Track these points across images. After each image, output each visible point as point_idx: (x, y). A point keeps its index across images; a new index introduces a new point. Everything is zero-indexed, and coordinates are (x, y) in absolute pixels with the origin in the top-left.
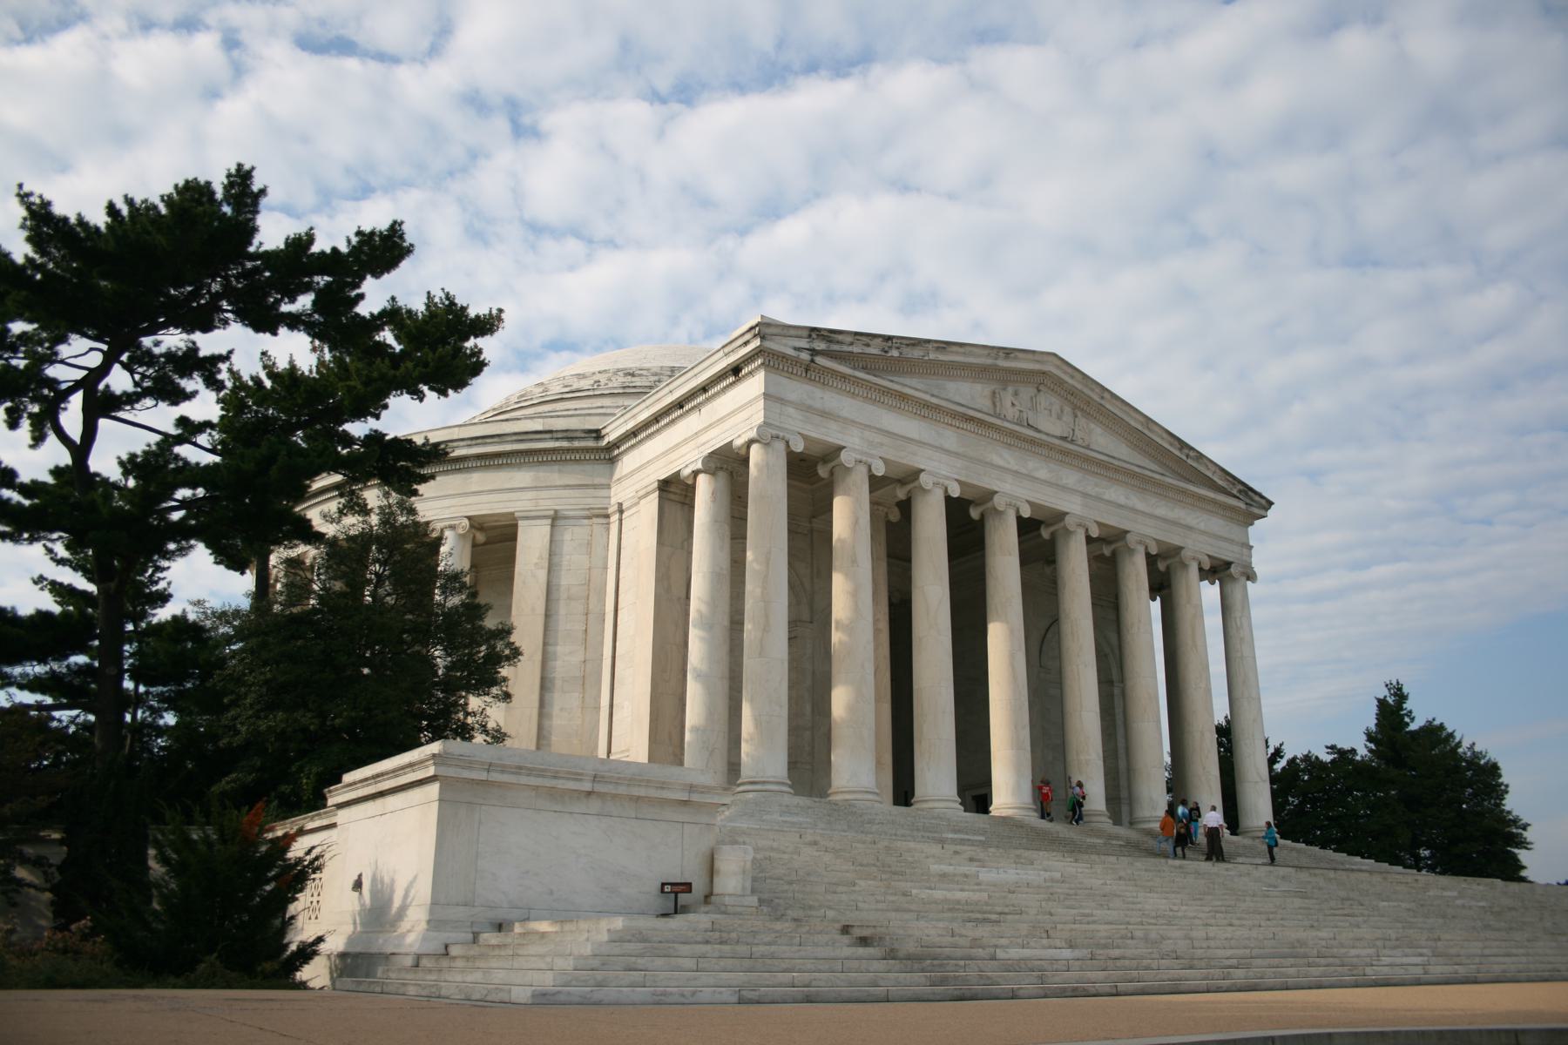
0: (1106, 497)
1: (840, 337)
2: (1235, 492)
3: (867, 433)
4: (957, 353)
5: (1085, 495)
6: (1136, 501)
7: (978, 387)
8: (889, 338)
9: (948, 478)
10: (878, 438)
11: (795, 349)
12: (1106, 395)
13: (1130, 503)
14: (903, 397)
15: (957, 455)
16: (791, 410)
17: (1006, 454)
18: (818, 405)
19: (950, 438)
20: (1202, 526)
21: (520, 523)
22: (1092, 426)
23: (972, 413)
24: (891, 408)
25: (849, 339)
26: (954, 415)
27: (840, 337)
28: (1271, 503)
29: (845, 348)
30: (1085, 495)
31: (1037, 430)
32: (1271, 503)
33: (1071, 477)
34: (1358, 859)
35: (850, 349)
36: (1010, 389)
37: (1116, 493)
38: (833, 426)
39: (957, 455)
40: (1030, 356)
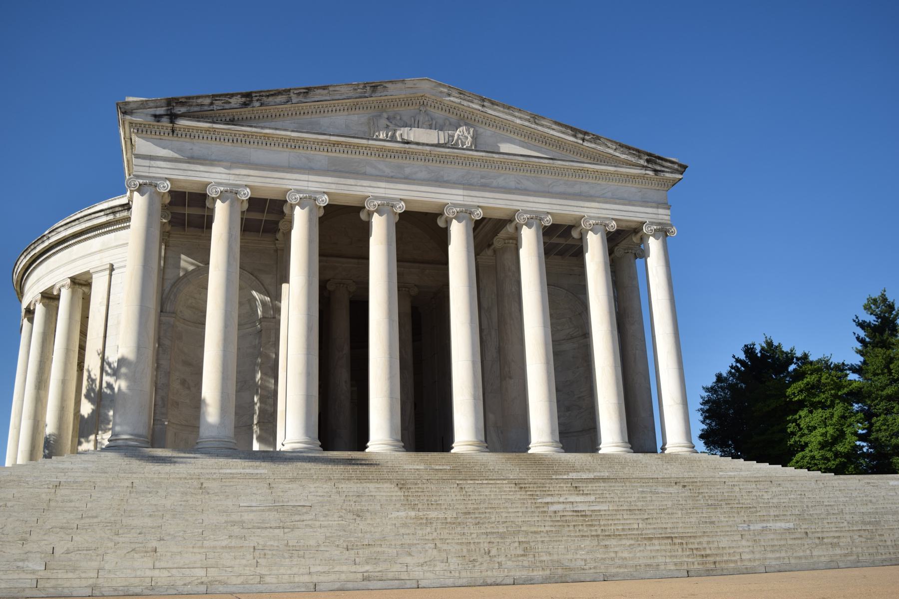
0: (495, 184)
1: (199, 101)
2: (642, 162)
4: (320, 94)
8: (248, 95)
11: (155, 116)
21: (94, 276)
25: (207, 101)
27: (199, 101)
28: (685, 167)
29: (206, 108)
31: (408, 143)
32: (685, 167)
34: (766, 466)
35: (211, 108)
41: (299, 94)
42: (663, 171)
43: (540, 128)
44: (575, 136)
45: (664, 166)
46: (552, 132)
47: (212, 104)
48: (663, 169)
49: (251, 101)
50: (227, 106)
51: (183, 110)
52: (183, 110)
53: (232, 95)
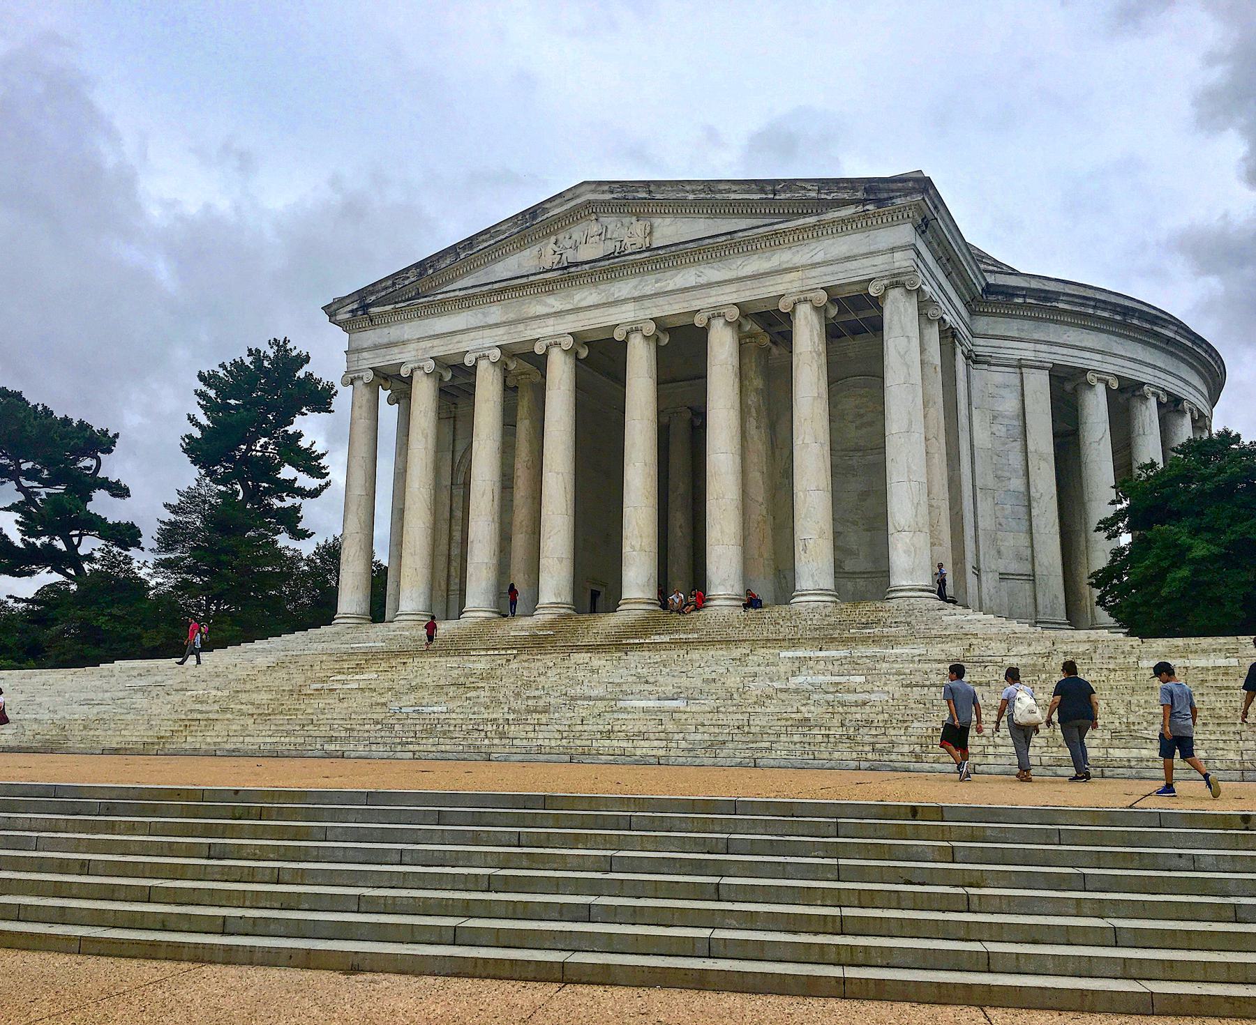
0: (669, 288)
2: (859, 195)
3: (423, 344)
4: (484, 241)
5: (635, 299)
6: (712, 273)
7: (527, 253)
9: (489, 348)
10: (428, 344)
11: (352, 311)
12: (652, 188)
13: (703, 280)
14: (443, 302)
15: (497, 325)
16: (365, 355)
17: (551, 300)
18: (385, 340)
19: (495, 313)
20: (819, 258)
22: (657, 221)
23: (496, 286)
24: (441, 315)
26: (490, 293)
30: (635, 299)
33: (624, 288)
36: (553, 239)
37: (686, 277)
38: (396, 350)
39: (497, 325)
40: (558, 201)
41: (464, 249)
42: (891, 198)
43: (718, 196)
44: (762, 191)
45: (893, 191)
46: (733, 196)
47: (394, 284)
48: (892, 195)
49: (426, 270)
50: (407, 282)
51: (373, 298)
52: (373, 298)
53: (407, 270)
